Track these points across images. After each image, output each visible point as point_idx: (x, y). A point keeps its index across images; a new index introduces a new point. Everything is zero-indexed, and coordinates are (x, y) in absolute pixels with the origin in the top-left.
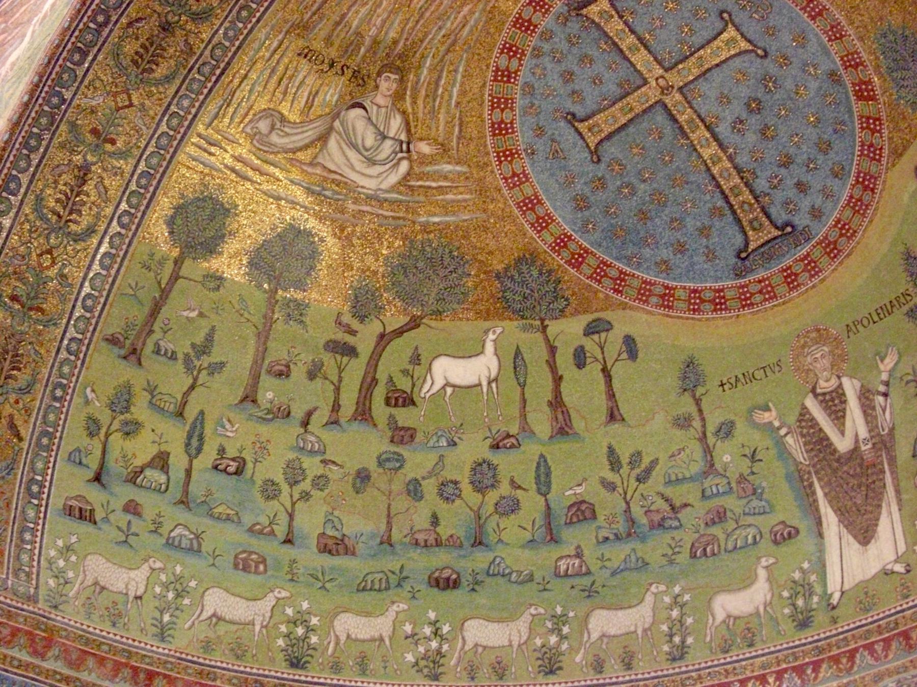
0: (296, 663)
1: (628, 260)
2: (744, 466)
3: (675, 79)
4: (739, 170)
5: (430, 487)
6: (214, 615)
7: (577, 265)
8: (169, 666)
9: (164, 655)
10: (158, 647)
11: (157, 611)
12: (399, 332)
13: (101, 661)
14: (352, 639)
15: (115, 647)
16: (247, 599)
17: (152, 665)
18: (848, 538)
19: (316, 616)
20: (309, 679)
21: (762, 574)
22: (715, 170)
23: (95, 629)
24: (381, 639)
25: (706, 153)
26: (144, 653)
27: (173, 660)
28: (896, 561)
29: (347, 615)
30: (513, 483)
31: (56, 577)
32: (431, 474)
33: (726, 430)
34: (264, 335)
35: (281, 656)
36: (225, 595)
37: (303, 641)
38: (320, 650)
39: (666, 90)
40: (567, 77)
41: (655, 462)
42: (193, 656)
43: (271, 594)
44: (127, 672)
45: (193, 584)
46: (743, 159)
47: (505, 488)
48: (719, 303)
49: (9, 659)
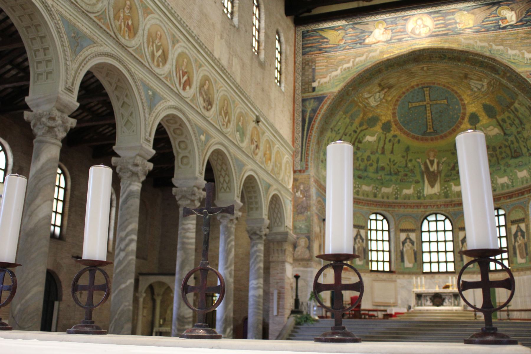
1: (404, 127)
2: (412, 168)
3: (431, 103)
4: (432, 119)
5: (360, 159)
7: (396, 125)
12: (364, 130)
18: (429, 186)
21: (412, 188)
22: (428, 118)
25: (428, 115)
28: (438, 192)
30: (373, 161)
32: (361, 156)
33: (411, 160)
34: (346, 128)
39: (427, 104)
40: (413, 96)
41: (397, 163)
46: (433, 118)
47: (371, 162)
48: (417, 139)
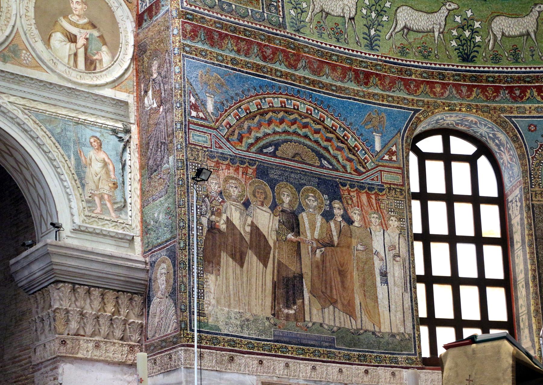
0: (466, 58)
6: (405, 27)
8: (379, 67)
9: (375, 60)
10: (370, 54)
11: (365, 27)
13: (334, 68)
14: (506, 36)
15: (341, 56)
16: (427, 13)
17: (367, 68)
19: (477, 21)
20: (477, 69)
23: (326, 44)
24: (528, 34)
26: (361, 59)
27: (381, 63)
29: (502, 18)
31: (295, 8)
35: (455, 53)
36: (411, 11)
37: (470, 41)
38: (483, 47)
42: (394, 59)
43: (444, 7)
44: (351, 74)
45: (388, 5)
49: (274, 71)
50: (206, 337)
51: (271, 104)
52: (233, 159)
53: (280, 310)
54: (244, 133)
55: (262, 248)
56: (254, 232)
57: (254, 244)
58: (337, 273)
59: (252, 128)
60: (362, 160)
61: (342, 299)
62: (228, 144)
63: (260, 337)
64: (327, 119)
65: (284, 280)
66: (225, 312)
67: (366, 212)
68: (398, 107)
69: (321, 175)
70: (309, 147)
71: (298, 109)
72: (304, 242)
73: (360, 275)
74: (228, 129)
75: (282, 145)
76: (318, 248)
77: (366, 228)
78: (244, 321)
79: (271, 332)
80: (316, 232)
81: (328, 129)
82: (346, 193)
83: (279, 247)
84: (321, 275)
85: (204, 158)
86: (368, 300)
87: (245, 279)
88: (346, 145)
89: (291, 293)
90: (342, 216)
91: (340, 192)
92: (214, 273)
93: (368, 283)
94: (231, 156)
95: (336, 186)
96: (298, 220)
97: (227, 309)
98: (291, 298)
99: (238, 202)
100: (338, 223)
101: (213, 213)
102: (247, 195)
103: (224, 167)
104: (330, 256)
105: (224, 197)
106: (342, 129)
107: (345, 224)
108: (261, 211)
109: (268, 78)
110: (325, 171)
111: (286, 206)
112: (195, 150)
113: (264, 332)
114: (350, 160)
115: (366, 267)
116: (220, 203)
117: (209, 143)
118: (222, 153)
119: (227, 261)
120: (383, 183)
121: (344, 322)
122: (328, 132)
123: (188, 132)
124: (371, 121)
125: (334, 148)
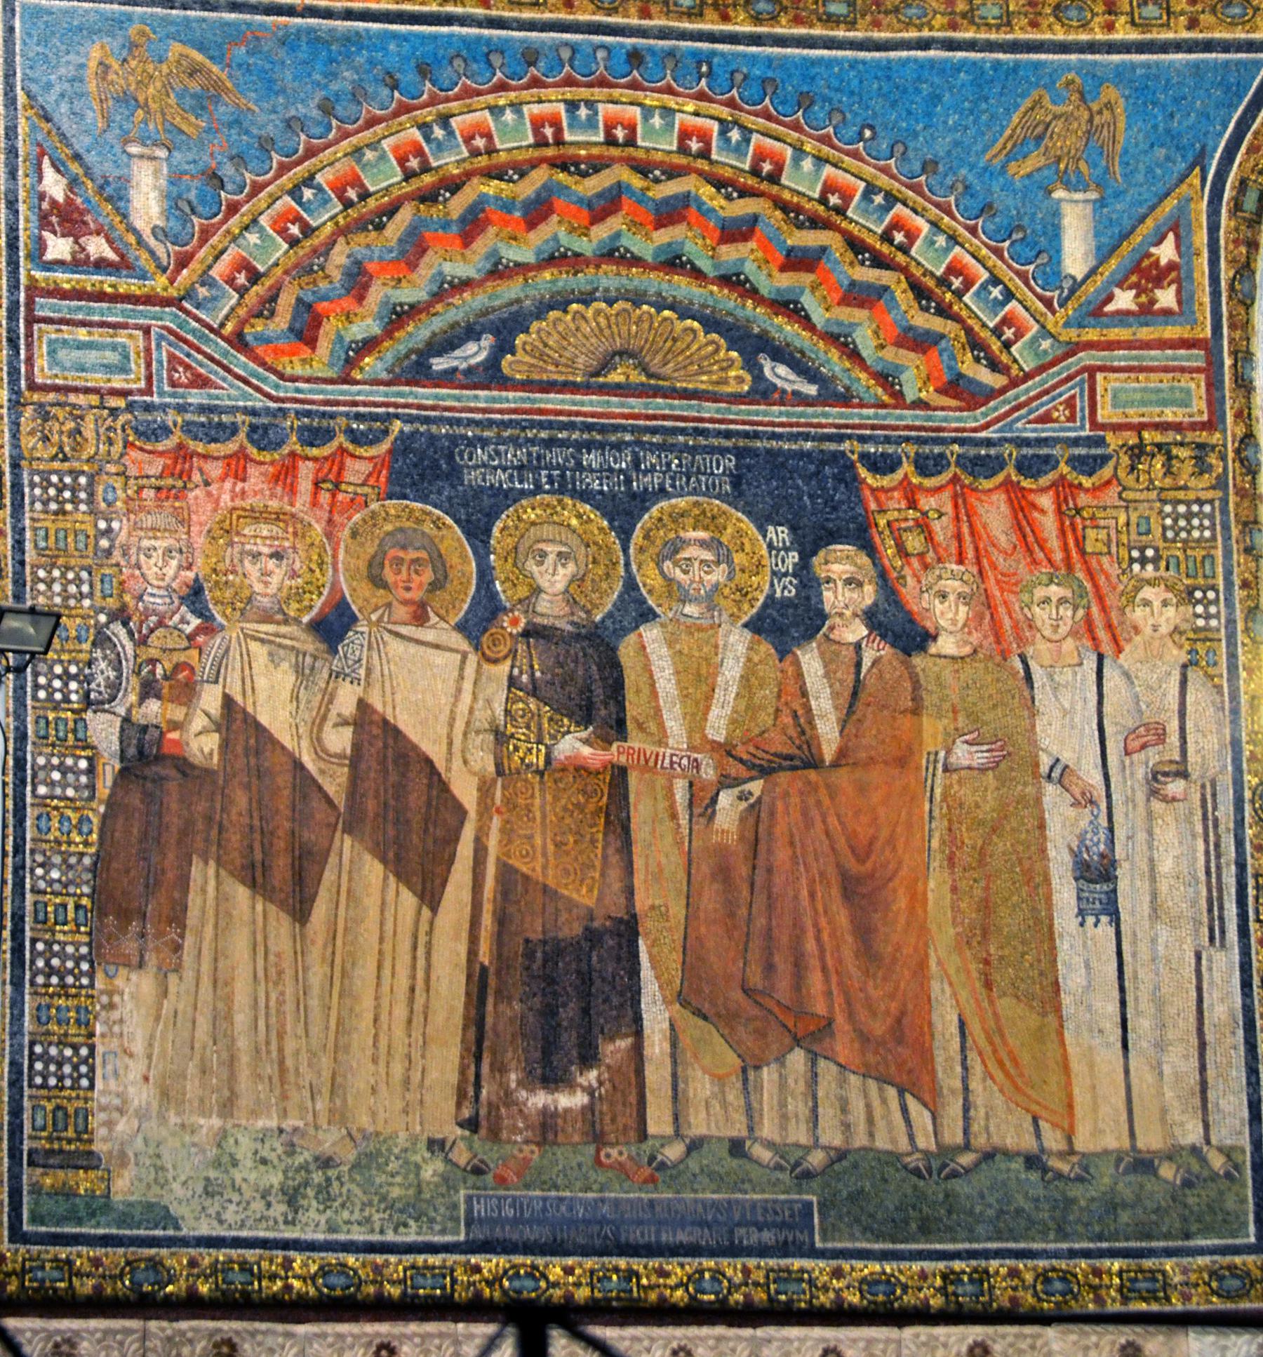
50: (96, 1262)
51: (480, 143)
52: (266, 428)
53: (508, 1098)
54: (325, 298)
55: (416, 820)
56: (371, 752)
57: (371, 805)
58: (835, 892)
59: (371, 267)
60: (985, 334)
61: (862, 1014)
62: (241, 363)
63: (390, 1237)
64: (797, 161)
65: (529, 955)
66: (202, 1136)
67: (1009, 583)
68: (1190, 47)
69: (756, 435)
70: (684, 312)
71: (631, 142)
72: (649, 765)
73: (963, 885)
74: (242, 291)
75: (535, 326)
76: (726, 781)
77: (1005, 655)
78: (304, 1167)
79: (455, 1206)
80: (715, 712)
81: (798, 210)
82: (896, 502)
83: (510, 804)
84: (743, 912)
85: (110, 442)
86: (1005, 1005)
87: (316, 976)
88: (904, 270)
89: (570, 1012)
90: (871, 617)
91: (862, 502)
92: (151, 959)
93: (1010, 920)
94: (253, 412)
95: (839, 479)
96: (616, 665)
97: (216, 1122)
98: (569, 1039)
99: (286, 622)
100: (848, 654)
101: (149, 690)
102: (335, 585)
103: (215, 470)
104: (796, 816)
105: (215, 611)
106: (879, 199)
107: (886, 651)
108: (413, 649)
109: (463, 21)
110: (776, 413)
111: (550, 609)
112: (60, 413)
113: (415, 1208)
114: (920, 342)
115: (1001, 845)
116: (191, 638)
117: (137, 367)
118: (202, 409)
119: (222, 898)
120: (1103, 427)
121: (870, 1120)
122: (800, 226)
123: (29, 335)
124: (1040, 138)
125: (837, 296)
